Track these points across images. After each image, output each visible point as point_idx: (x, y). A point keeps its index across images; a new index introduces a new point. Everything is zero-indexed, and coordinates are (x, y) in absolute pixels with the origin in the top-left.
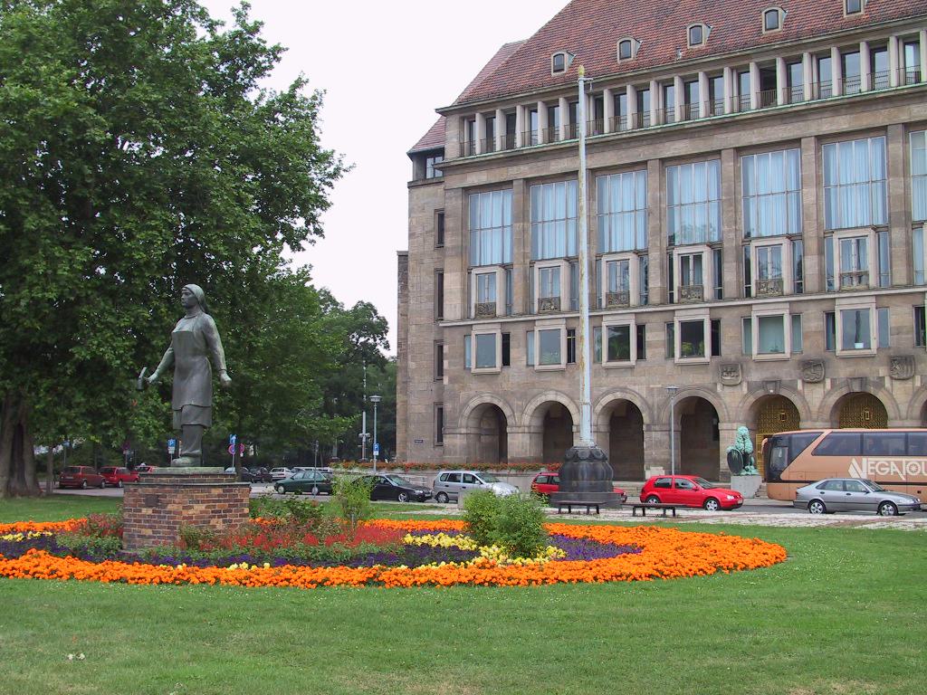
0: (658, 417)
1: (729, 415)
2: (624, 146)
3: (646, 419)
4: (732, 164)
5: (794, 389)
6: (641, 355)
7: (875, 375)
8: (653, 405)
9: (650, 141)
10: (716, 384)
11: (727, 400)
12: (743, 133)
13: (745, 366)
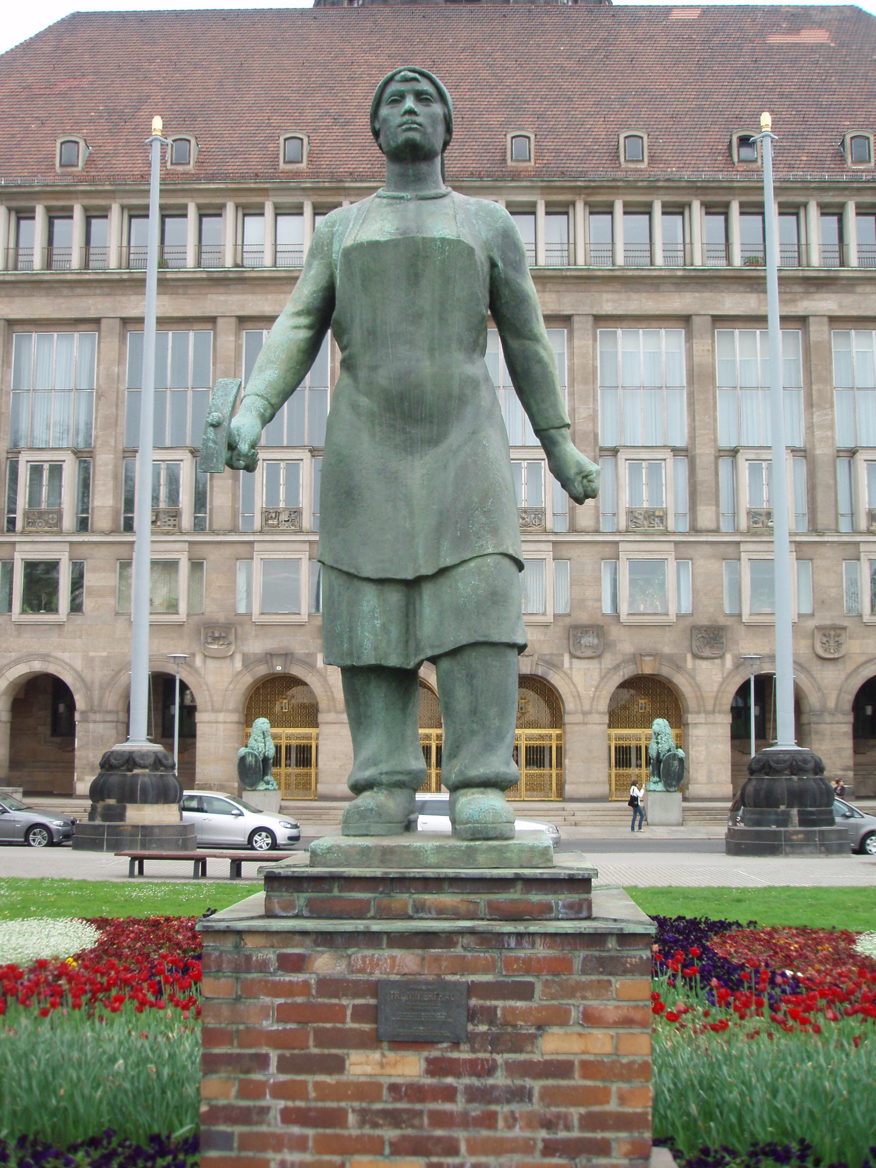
0: (101, 700)
1: (212, 701)
2: (65, 292)
3: (80, 702)
4: (232, 338)
5: (312, 666)
6: (76, 607)
8: (93, 683)
9: (107, 290)
10: (193, 655)
11: (211, 678)
12: (250, 297)
13: (240, 630)
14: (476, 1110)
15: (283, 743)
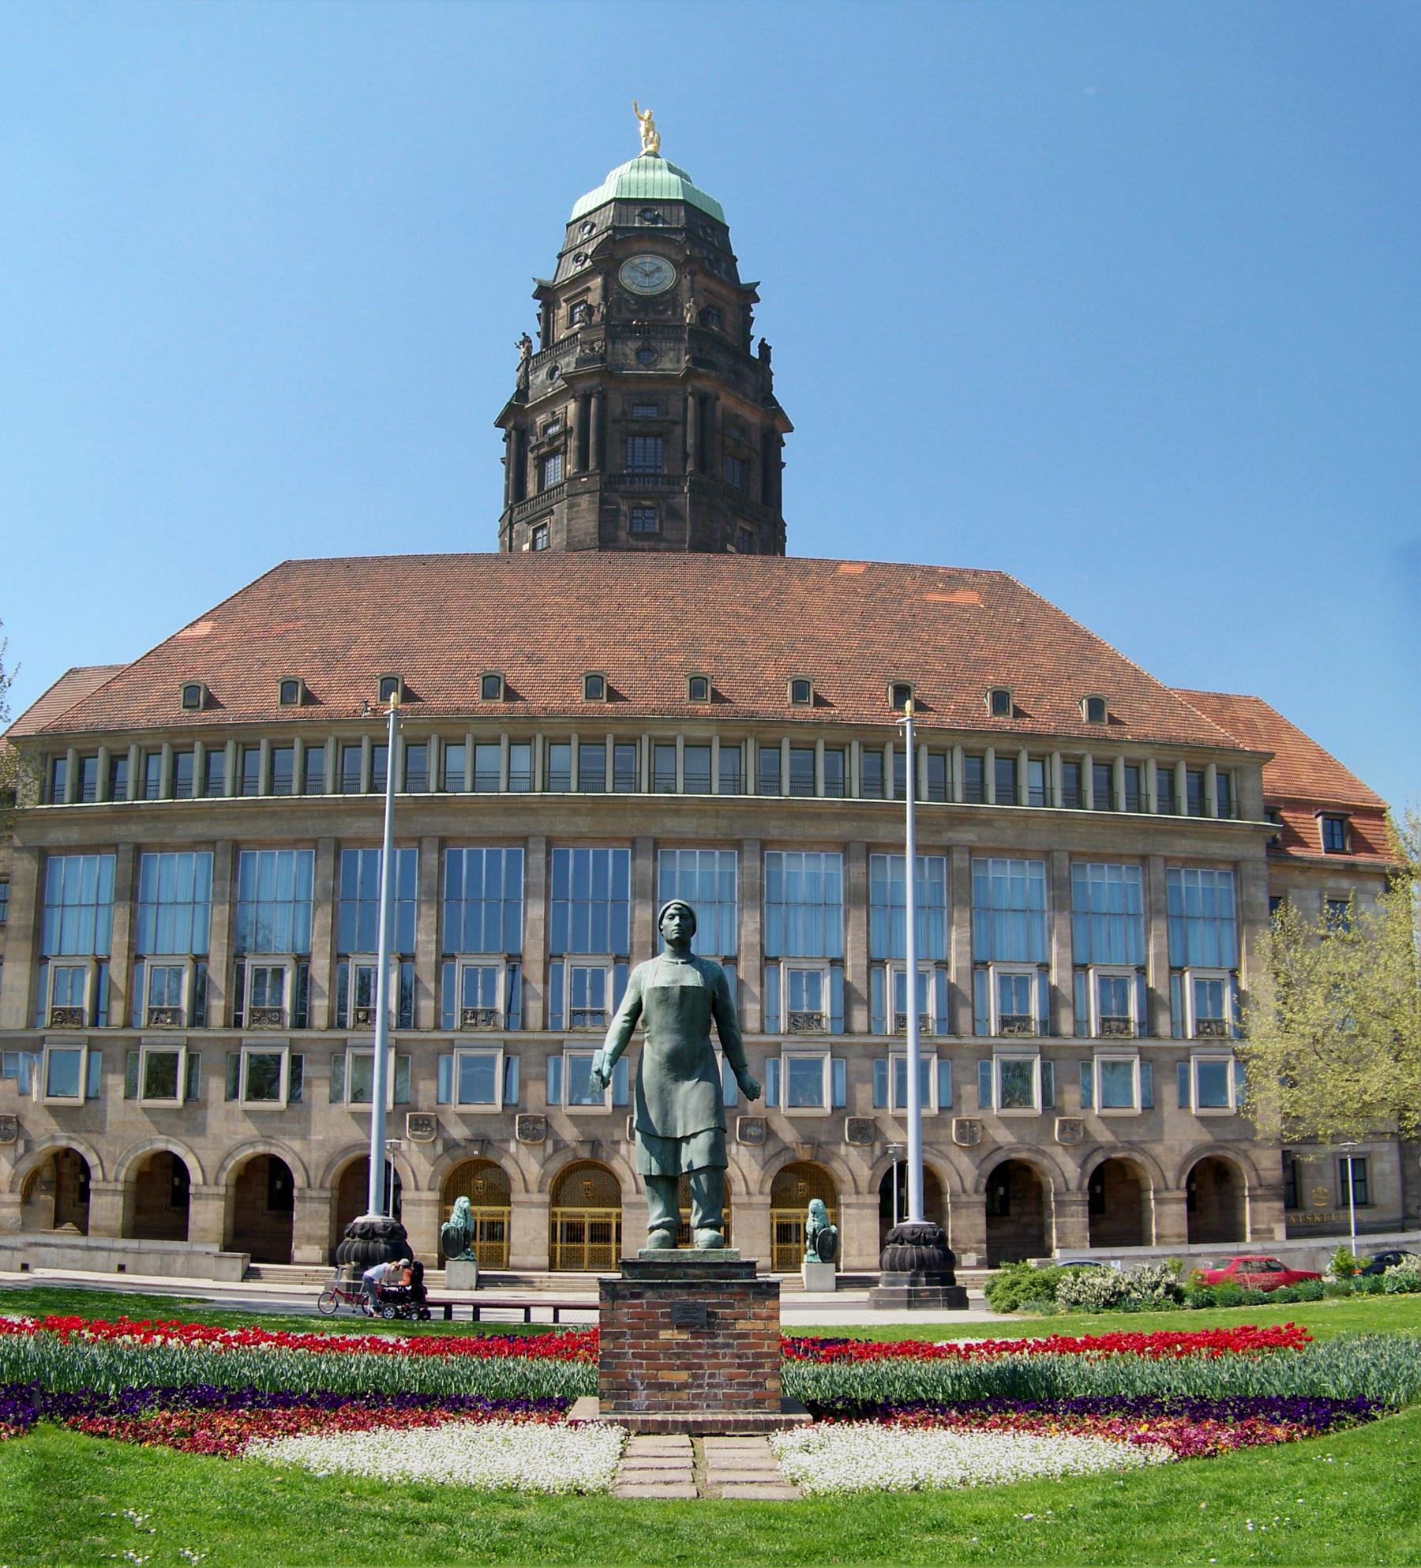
3: (299, 1179)
4: (436, 856)
7: (610, 1139)
14: (710, 1352)
15: (479, 1218)
